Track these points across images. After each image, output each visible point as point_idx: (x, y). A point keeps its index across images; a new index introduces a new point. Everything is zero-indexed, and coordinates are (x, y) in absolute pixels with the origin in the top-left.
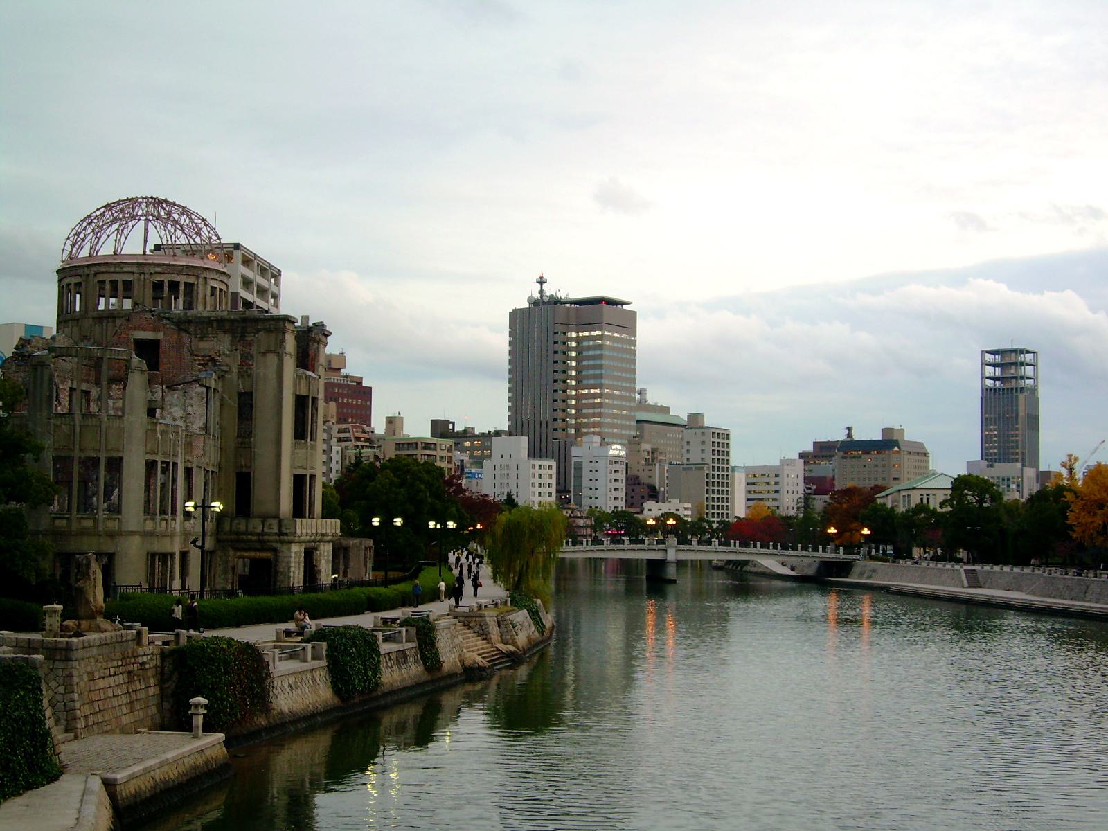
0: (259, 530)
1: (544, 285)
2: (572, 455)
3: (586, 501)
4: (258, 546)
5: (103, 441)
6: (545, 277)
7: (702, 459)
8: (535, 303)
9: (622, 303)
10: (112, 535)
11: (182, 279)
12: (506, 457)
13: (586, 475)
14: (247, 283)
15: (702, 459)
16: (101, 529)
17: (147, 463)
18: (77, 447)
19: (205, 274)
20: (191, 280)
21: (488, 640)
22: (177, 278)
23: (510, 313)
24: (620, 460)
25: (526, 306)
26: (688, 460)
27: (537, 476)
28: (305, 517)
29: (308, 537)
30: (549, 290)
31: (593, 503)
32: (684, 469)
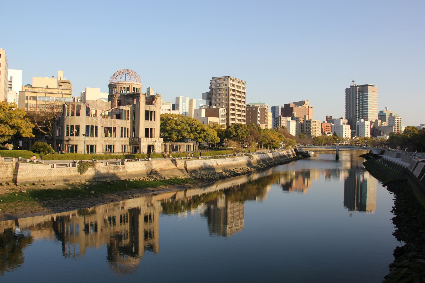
0: (135, 140)
1: (354, 82)
2: (357, 124)
3: (359, 135)
4: (136, 144)
5: (75, 122)
6: (354, 80)
7: (393, 125)
8: (352, 86)
9: (374, 86)
10: (77, 141)
11: (126, 86)
12: (337, 125)
13: (360, 129)
14: (233, 85)
15: (393, 125)
16: (75, 139)
17: (86, 126)
18: (75, 123)
19: (131, 85)
20: (128, 86)
21: (177, 167)
22: (125, 86)
23: (347, 90)
24: (368, 125)
25: (350, 87)
26: (389, 125)
27: (345, 129)
28: (148, 137)
29: (149, 142)
30: (355, 83)
31: (361, 135)
32: (388, 127)
